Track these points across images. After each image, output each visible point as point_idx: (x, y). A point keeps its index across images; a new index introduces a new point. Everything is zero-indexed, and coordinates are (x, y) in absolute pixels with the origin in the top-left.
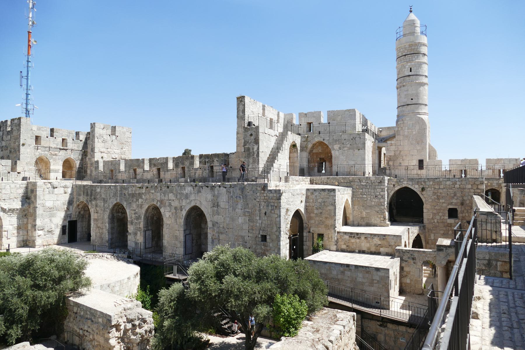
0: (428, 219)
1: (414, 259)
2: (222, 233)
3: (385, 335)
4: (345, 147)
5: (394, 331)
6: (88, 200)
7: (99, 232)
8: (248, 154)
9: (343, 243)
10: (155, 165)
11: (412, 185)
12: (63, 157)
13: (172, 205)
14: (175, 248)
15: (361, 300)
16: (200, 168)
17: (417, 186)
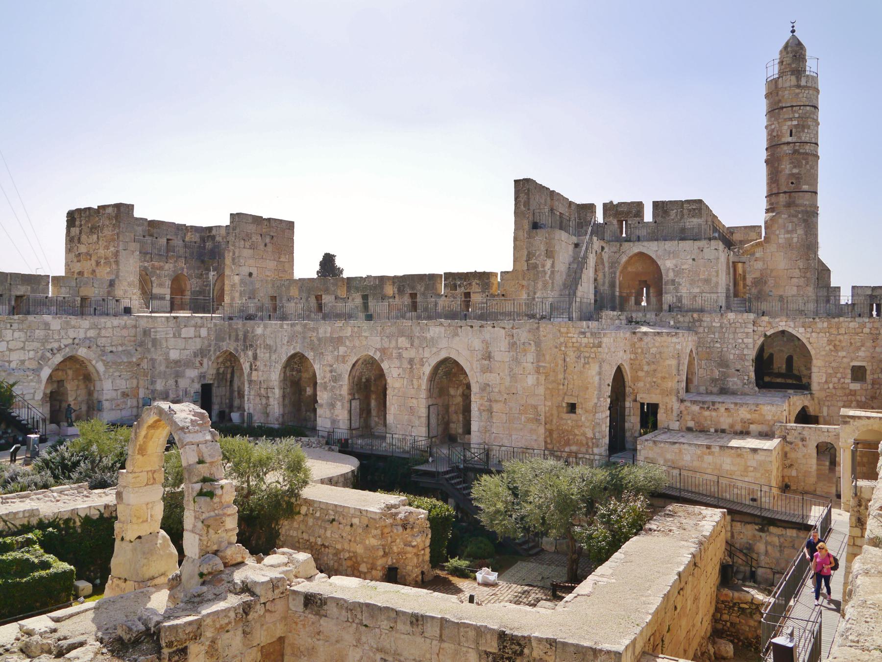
0: (819, 383)
1: (803, 440)
2: (496, 401)
3: (767, 543)
4: (685, 263)
5: (779, 536)
6: (239, 348)
7: (261, 404)
8: (534, 275)
9: (690, 417)
10: (357, 289)
11: (794, 328)
12: (171, 273)
13: (404, 356)
14: (410, 427)
15: (728, 497)
16: (446, 296)
17: (802, 330)
